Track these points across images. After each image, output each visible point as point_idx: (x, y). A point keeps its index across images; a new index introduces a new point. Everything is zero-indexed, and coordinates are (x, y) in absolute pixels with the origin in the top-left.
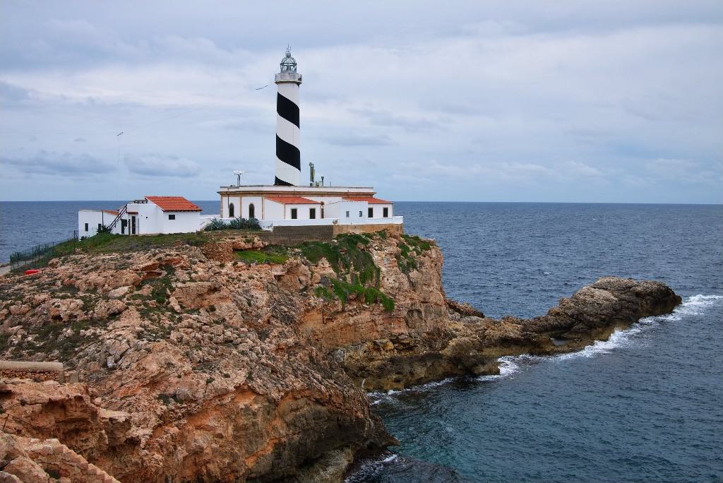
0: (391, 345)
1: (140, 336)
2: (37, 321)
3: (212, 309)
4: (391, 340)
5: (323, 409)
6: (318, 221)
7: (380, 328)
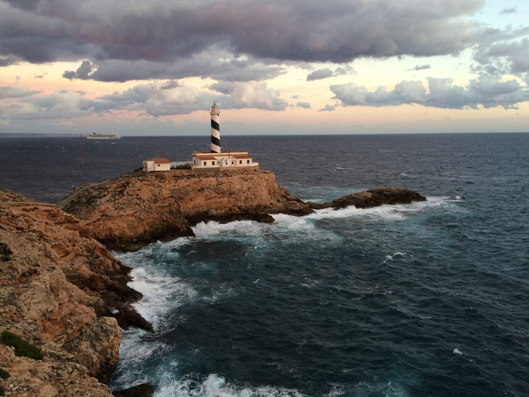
0: (237, 209)
1: (108, 201)
2: (89, 197)
3: (138, 195)
4: (239, 208)
5: (165, 224)
6: (216, 166)
7: (232, 203)
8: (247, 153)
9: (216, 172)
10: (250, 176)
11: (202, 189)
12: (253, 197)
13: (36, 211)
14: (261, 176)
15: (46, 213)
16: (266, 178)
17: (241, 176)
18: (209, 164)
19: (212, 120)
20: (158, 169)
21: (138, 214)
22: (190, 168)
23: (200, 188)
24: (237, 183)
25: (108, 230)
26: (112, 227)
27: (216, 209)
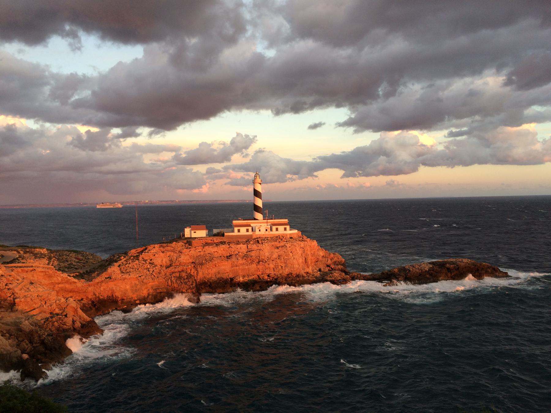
0: (266, 277)
3: (151, 260)
4: (268, 276)
6: (250, 233)
8: (286, 221)
9: (248, 240)
10: (282, 244)
11: (230, 256)
12: (283, 265)
13: (33, 272)
14: (295, 244)
15: (42, 274)
16: (302, 245)
17: (273, 243)
18: (243, 230)
19: (254, 189)
20: (194, 235)
21: (142, 277)
22: (223, 235)
23: (228, 255)
24: (266, 250)
25: (110, 292)
26: (114, 288)
27: (244, 276)
